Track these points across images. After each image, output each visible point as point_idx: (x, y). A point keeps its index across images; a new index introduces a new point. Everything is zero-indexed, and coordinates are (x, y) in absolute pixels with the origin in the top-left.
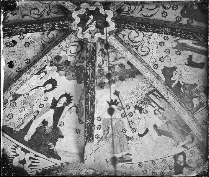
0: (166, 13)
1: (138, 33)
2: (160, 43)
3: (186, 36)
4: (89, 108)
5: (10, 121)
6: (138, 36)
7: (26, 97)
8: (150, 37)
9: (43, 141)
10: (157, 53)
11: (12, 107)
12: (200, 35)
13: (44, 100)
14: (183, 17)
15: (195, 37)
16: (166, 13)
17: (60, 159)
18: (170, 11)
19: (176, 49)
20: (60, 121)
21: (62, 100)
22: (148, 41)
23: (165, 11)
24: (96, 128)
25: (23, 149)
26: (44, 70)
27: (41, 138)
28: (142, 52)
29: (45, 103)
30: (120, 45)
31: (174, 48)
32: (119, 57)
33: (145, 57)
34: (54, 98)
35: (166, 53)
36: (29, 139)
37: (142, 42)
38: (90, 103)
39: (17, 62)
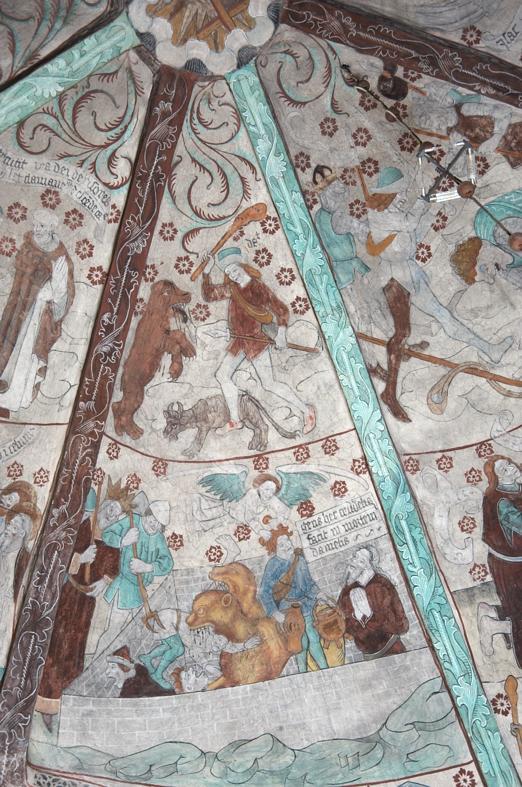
0: (172, 238)
1: (110, 129)
2: (56, 193)
3: (114, 302)
6: (95, 123)
8: (87, 165)
10: (16, 178)
12: (119, 345)
14: (153, 288)
15: (109, 328)
16: (172, 238)
18: (174, 249)
19: (22, 242)
22: (71, 156)
23: (179, 236)
28: (35, 129)
30: (94, 62)
31: (28, 237)
32: (15, 25)
33: (15, 140)
35: (10, 208)
37: (68, 130)
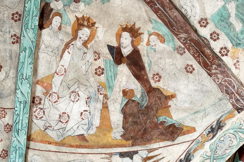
4: (165, 15)
5: (71, 124)
7: (63, 72)
9: (145, 123)
11: (55, 102)
13: (95, 60)
17: (193, 130)
20: (150, 76)
21: (123, 40)
24: (210, 40)
25: (122, 155)
26: (52, 13)
27: (138, 120)
29: (100, 63)
34: (108, 46)
36: (122, 133)
38: (159, 4)
39: (3, 30)
